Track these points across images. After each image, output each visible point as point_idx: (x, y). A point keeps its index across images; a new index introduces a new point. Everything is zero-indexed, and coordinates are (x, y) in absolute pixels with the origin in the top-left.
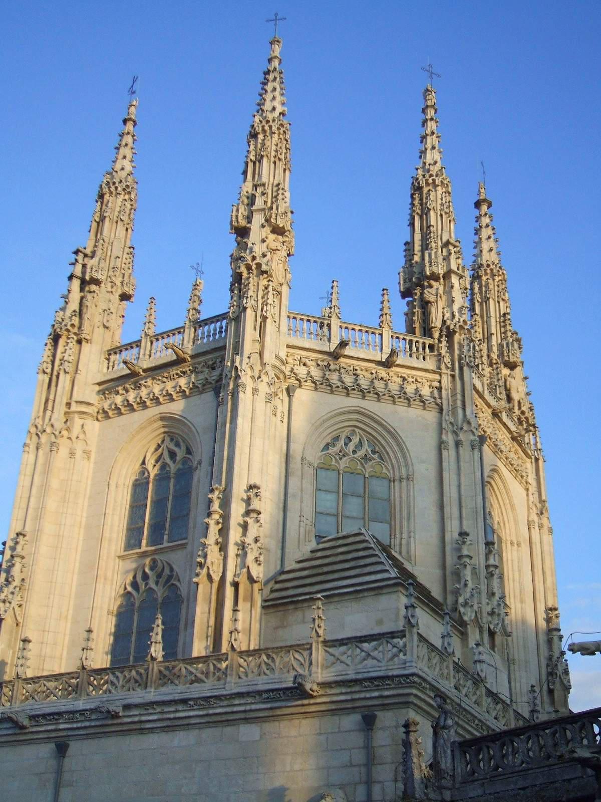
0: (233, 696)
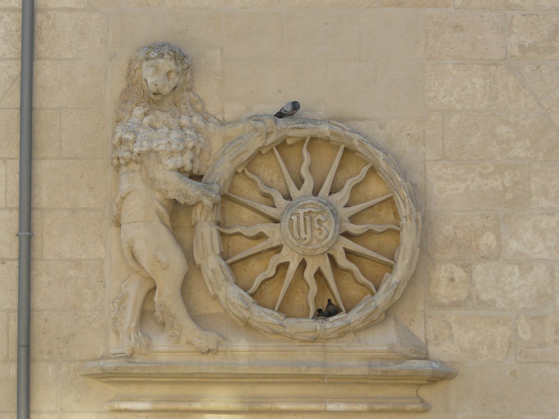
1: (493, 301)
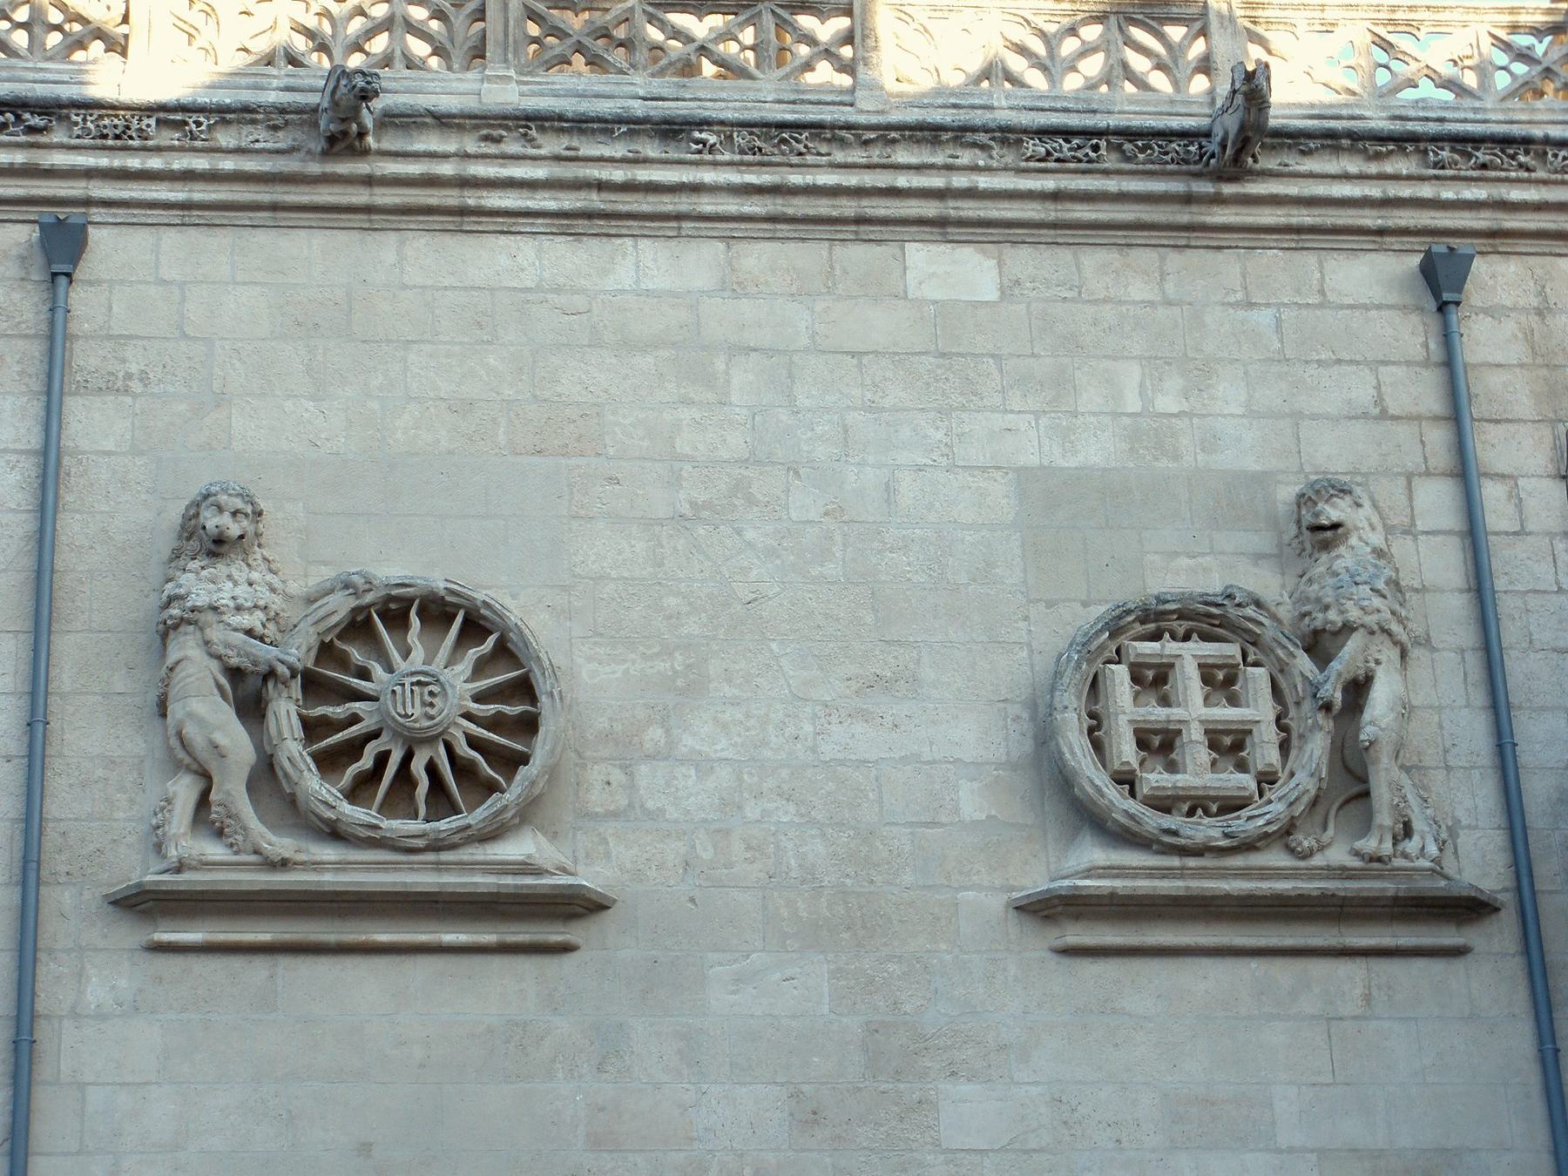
0: (893, 135)
1: (662, 811)
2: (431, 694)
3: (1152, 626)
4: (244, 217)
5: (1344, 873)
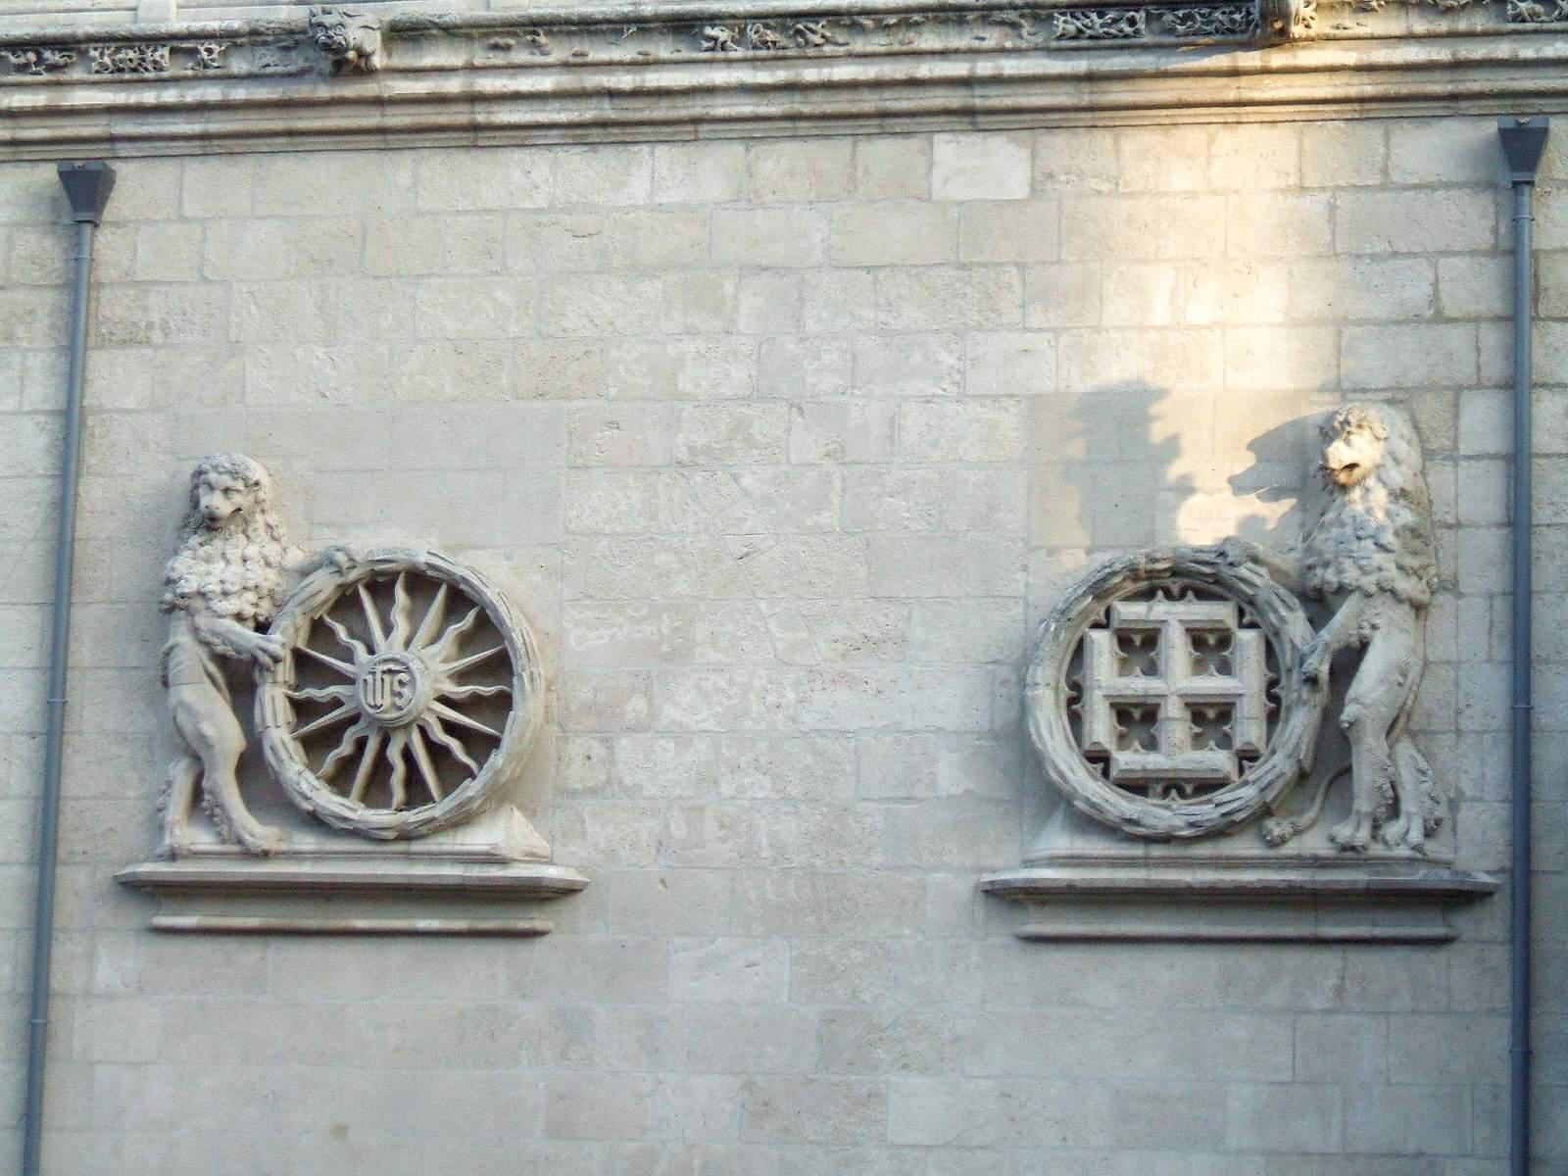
0: (916, 17)
1: (640, 787)
2: (401, 682)
3: (1143, 585)
4: (262, 144)
5: (1317, 862)
